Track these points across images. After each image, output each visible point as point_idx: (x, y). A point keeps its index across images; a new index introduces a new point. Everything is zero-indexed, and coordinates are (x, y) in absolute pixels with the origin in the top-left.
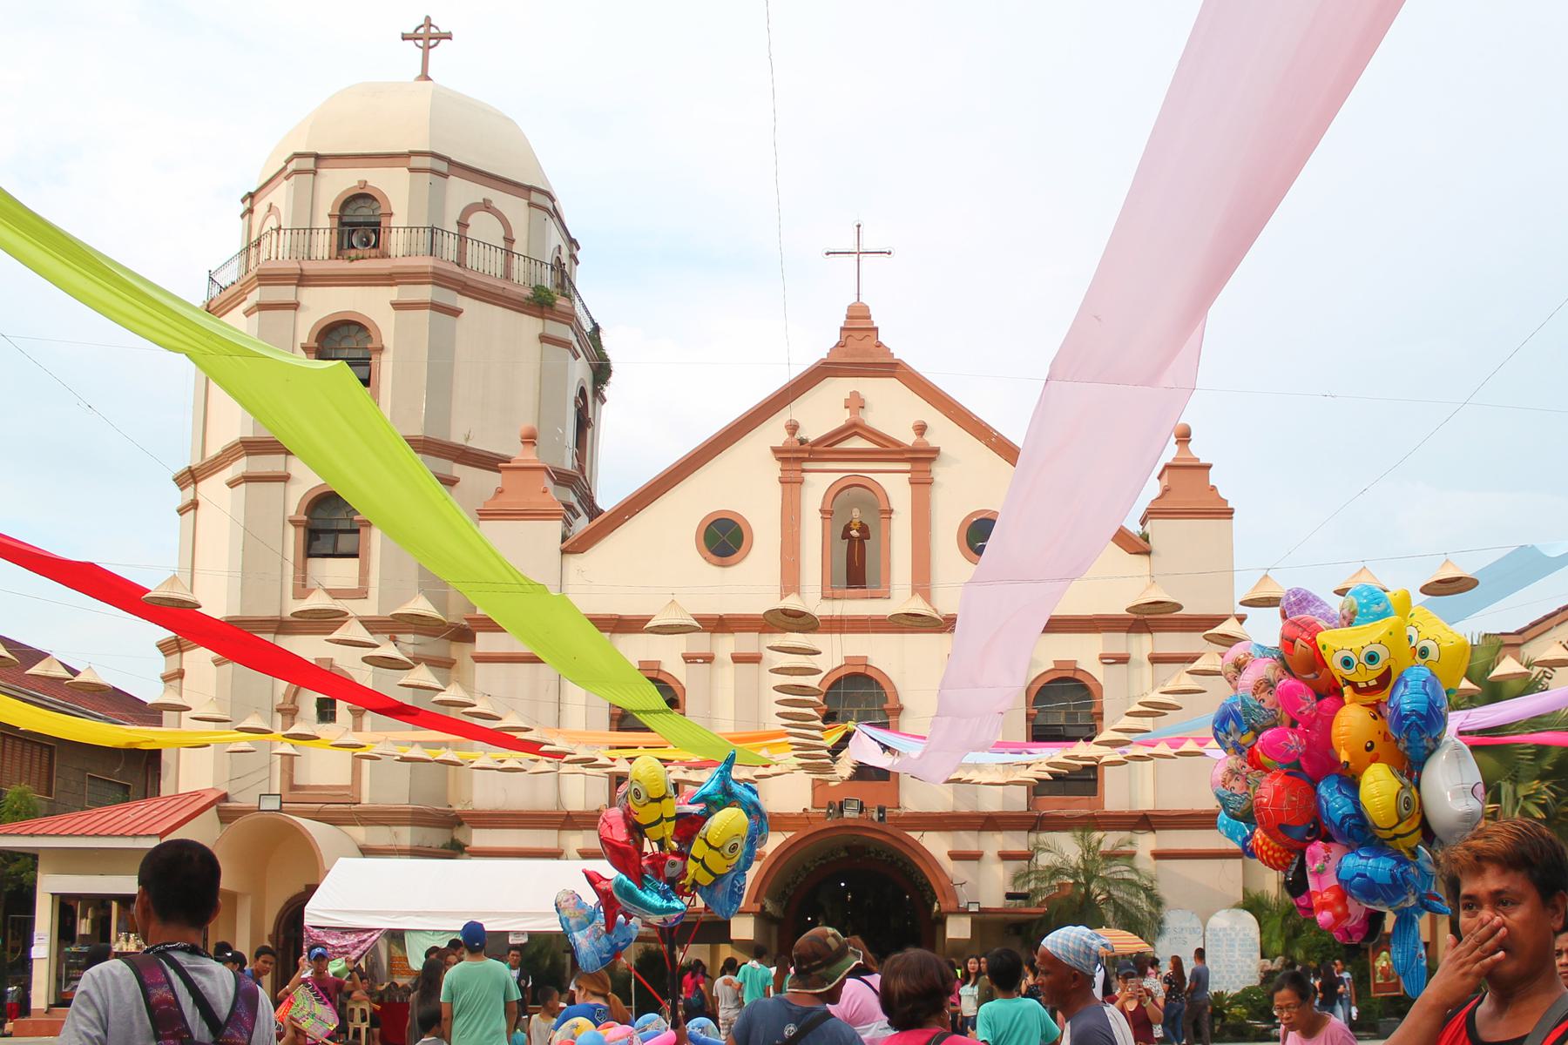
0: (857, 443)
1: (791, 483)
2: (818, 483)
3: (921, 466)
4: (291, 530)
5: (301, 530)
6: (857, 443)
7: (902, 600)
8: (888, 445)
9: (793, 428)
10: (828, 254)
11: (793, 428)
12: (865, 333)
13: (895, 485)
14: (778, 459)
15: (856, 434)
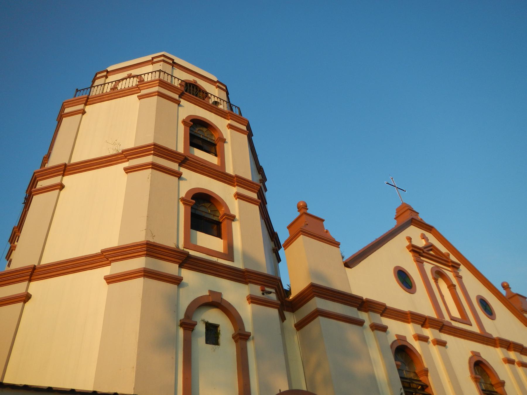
0: (431, 252)
1: (420, 263)
2: (428, 266)
3: (456, 270)
4: (182, 207)
5: (189, 208)
6: (431, 252)
7: (475, 328)
8: (443, 256)
9: (409, 239)
10: (387, 183)
11: (409, 239)
12: (416, 214)
13: (450, 275)
14: (410, 251)
15: (431, 250)
